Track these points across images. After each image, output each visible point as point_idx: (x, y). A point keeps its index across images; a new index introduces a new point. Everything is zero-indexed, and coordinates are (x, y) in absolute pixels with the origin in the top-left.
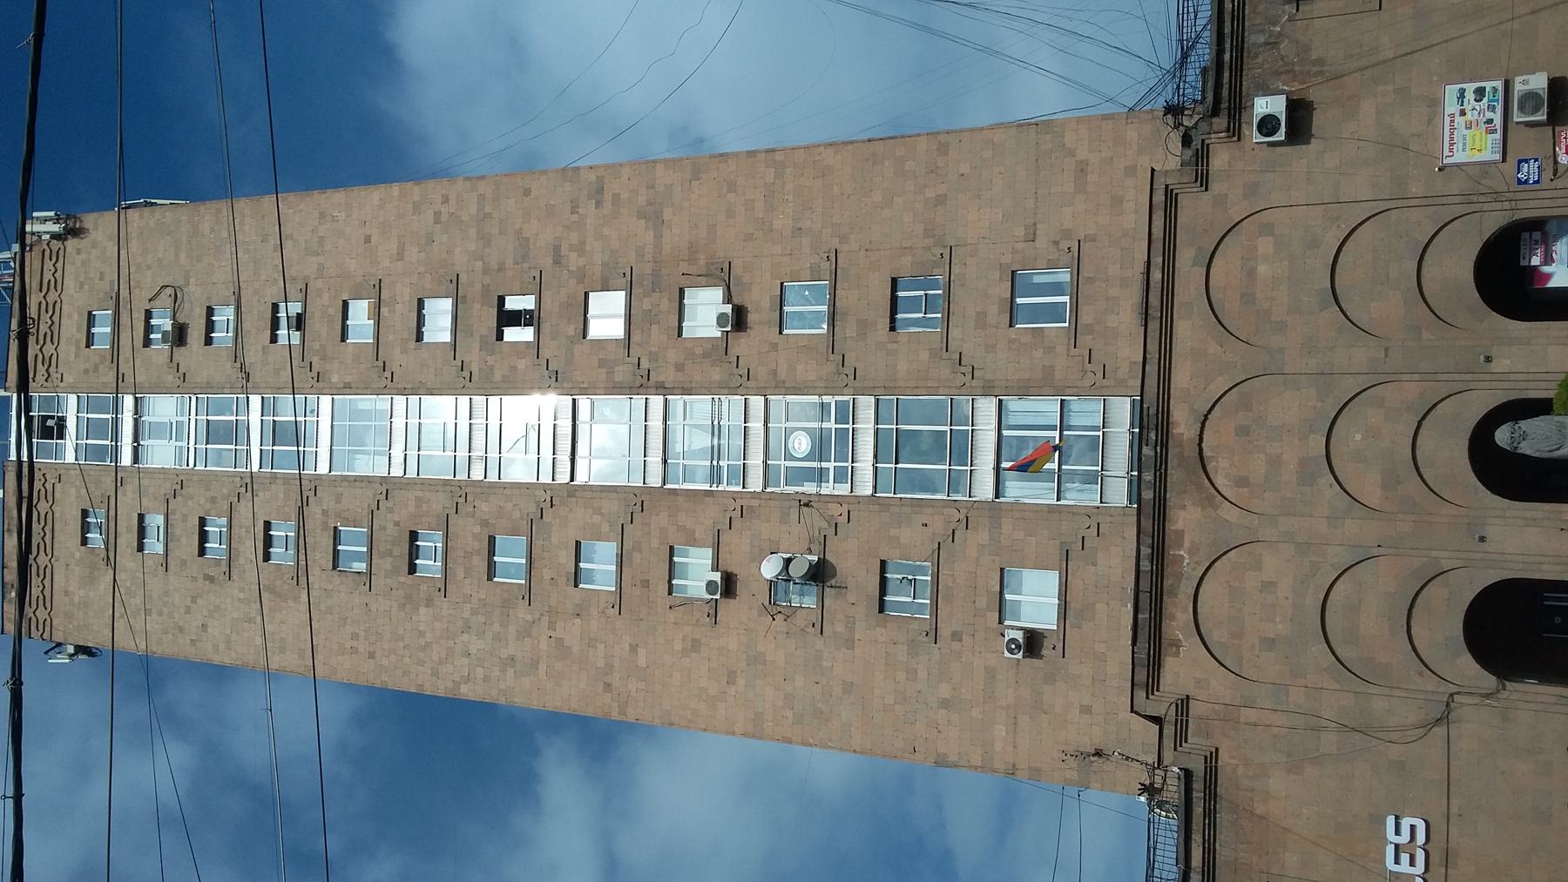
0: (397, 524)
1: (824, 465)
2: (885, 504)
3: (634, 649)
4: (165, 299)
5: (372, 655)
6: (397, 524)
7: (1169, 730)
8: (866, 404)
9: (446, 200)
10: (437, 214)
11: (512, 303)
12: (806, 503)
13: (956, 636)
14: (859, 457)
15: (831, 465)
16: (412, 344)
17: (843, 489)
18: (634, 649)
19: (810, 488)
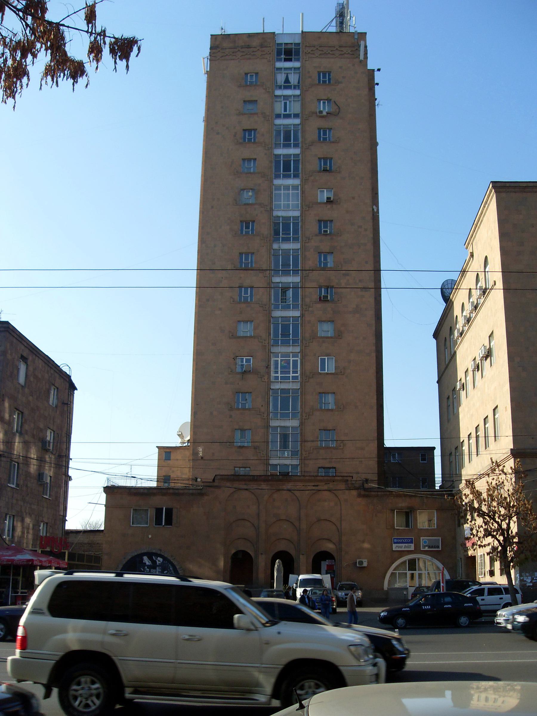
0: (257, 215)
1: (279, 372)
2: (268, 394)
3: (220, 309)
4: (334, 109)
5: (212, 207)
6: (257, 215)
7: (211, 484)
8: (297, 386)
9: (366, 230)
10: (360, 227)
11: (330, 259)
12: (268, 367)
13: (231, 416)
14: (282, 384)
15: (279, 375)
16: (317, 218)
17: (272, 379)
18: (220, 309)
19: (272, 367)
